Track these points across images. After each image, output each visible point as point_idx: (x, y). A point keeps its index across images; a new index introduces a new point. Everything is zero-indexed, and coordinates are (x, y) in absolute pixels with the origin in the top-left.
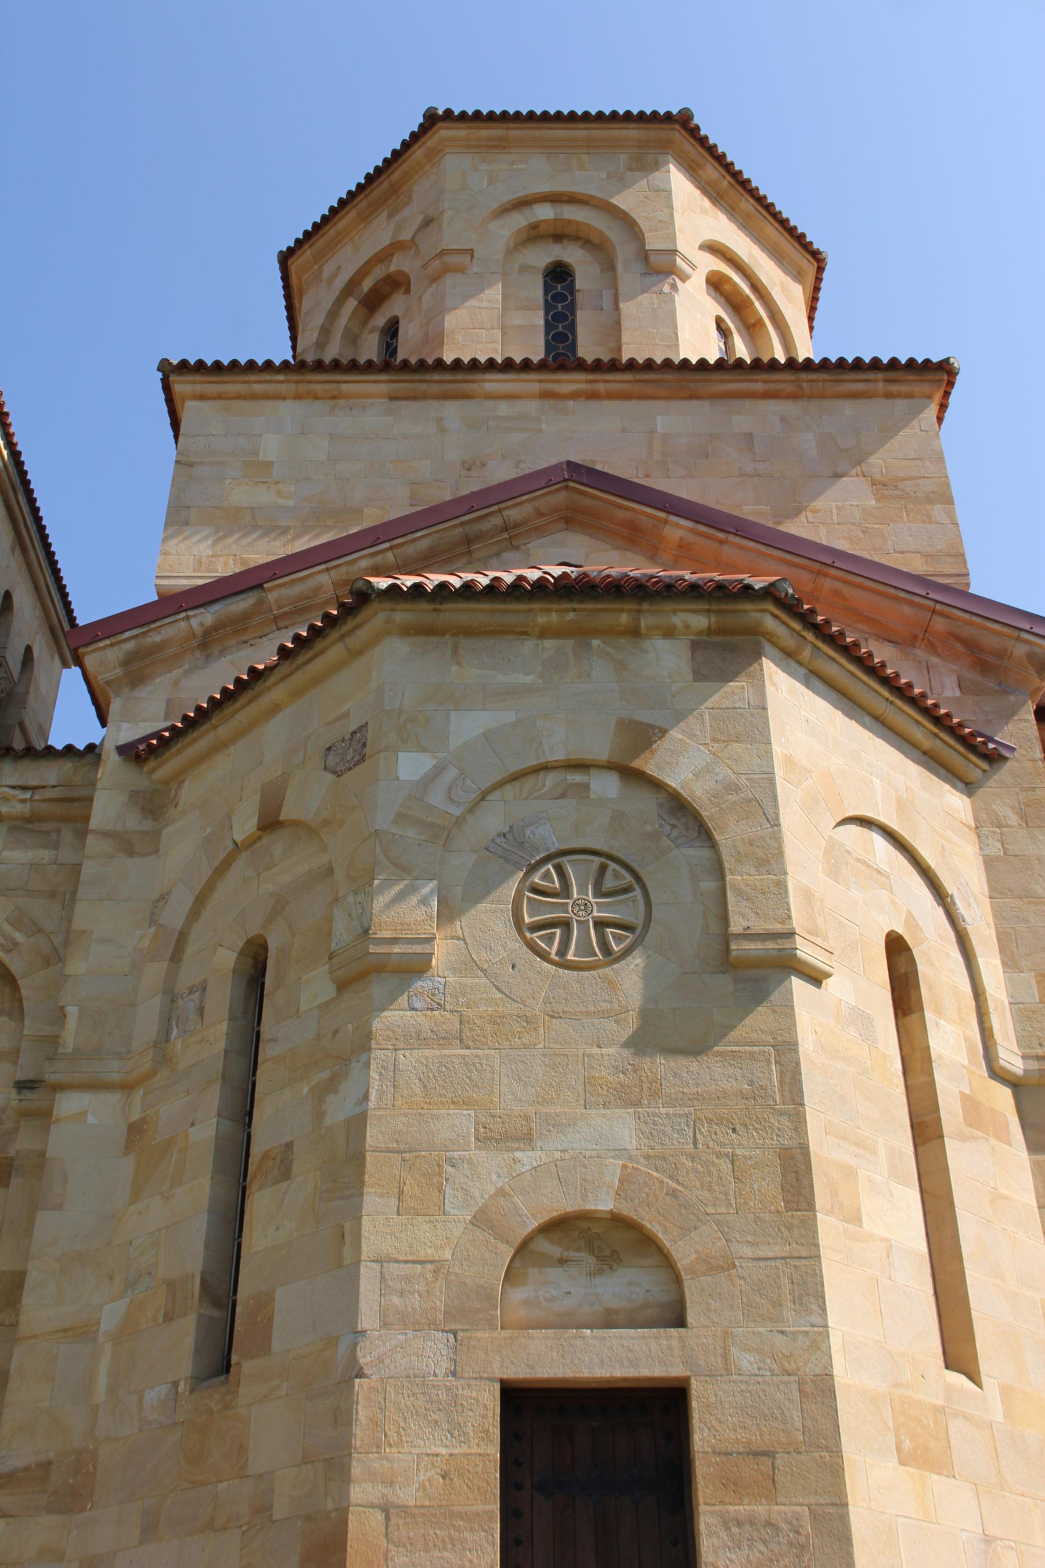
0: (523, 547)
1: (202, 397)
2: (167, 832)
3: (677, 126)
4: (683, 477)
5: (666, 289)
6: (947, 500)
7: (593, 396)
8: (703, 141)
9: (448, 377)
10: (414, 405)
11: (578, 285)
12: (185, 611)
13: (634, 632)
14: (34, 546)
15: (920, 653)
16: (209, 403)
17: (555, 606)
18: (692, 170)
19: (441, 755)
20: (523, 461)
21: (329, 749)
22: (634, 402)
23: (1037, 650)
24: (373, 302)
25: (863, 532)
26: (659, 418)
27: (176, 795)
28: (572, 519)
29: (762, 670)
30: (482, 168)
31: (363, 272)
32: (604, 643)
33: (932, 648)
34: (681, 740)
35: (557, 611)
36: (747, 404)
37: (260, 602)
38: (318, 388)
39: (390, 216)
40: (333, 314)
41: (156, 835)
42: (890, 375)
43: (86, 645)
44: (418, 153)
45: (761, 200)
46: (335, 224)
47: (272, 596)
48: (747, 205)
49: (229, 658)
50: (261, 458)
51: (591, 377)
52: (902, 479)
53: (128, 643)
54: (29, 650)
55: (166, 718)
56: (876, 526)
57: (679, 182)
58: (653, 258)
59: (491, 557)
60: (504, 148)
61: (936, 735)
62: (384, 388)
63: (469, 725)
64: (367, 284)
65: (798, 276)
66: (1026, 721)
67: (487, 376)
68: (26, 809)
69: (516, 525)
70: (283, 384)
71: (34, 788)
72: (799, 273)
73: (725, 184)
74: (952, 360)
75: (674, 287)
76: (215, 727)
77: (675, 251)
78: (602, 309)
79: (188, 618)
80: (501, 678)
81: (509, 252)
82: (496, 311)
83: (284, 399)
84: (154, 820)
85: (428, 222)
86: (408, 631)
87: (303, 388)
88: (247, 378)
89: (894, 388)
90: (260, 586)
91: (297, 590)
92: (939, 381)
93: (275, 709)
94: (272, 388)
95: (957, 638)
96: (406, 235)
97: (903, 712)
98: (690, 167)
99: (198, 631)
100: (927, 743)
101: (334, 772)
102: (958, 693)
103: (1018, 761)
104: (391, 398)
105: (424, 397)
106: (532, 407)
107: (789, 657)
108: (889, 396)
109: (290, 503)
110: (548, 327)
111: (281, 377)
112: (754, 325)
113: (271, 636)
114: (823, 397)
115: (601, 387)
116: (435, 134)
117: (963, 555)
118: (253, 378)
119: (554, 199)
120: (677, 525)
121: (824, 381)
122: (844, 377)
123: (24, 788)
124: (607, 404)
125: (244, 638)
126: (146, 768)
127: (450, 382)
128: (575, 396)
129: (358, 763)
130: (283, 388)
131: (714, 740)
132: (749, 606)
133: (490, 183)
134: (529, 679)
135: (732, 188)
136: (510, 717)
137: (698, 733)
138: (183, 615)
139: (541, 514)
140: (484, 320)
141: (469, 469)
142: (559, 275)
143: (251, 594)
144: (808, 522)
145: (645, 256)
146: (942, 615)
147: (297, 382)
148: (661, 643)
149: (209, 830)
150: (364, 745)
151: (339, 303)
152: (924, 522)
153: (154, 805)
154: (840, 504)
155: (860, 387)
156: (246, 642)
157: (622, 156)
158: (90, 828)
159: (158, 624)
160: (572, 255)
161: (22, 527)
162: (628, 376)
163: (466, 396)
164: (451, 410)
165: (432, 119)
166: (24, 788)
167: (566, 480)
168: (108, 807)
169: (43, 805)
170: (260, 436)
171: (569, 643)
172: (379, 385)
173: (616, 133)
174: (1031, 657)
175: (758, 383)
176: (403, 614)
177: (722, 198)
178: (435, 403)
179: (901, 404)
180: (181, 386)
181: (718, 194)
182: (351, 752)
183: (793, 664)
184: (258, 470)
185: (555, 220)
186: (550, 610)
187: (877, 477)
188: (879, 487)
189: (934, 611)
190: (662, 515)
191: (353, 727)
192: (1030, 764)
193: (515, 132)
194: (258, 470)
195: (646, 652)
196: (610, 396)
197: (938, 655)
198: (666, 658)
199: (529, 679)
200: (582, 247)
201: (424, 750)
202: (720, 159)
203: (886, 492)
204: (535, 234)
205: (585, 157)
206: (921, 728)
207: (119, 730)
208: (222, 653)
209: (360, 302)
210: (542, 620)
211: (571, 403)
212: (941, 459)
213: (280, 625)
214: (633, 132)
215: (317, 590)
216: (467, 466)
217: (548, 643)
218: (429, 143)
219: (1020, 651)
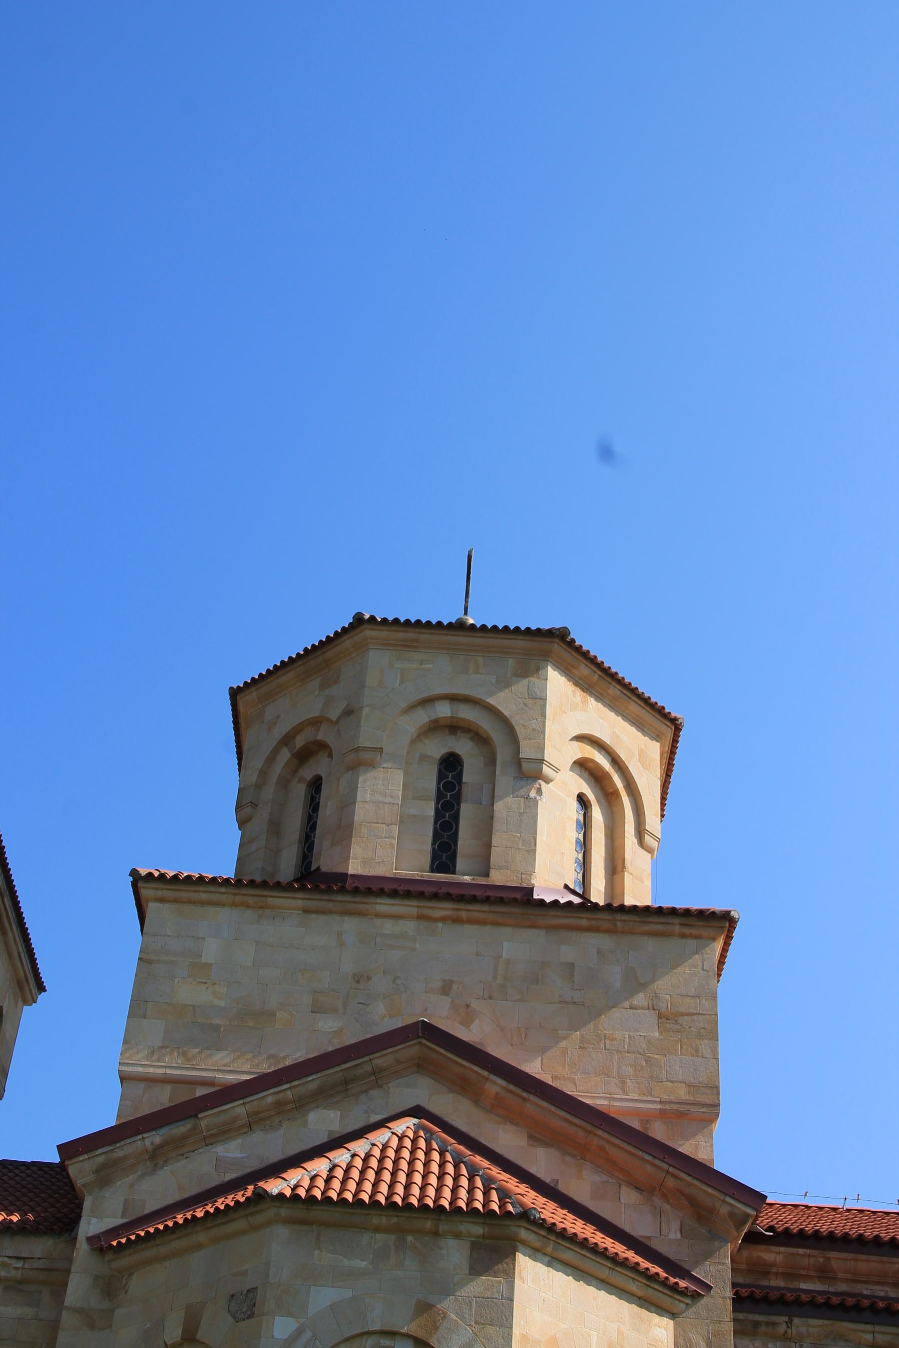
0: (385, 1086)
1: (161, 900)
2: (119, 1312)
3: (557, 640)
4: (516, 1001)
5: (533, 794)
6: (713, 1035)
7: (457, 921)
8: (579, 649)
9: (348, 898)
10: (322, 918)
11: (465, 779)
12: (142, 1133)
13: (436, 1233)
14: (12, 929)
15: (657, 1201)
16: (167, 905)
17: (385, 1213)
18: (567, 671)
19: (302, 1320)
20: (399, 978)
21: (232, 1296)
22: (488, 927)
23: (736, 1211)
24: (304, 756)
25: (646, 1061)
26: (505, 944)
27: (126, 1284)
28: (422, 1066)
29: (514, 1269)
30: (397, 666)
31: (298, 730)
32: (415, 1239)
33: (665, 1197)
34: (455, 1321)
35: (386, 1216)
36: (574, 936)
37: (195, 1128)
38: (251, 901)
39: (323, 686)
40: (271, 759)
41: (112, 1311)
42: (684, 920)
43: (70, 1158)
44: (347, 643)
45: (627, 687)
46: (278, 678)
47: (203, 1124)
48: (614, 690)
49: (170, 1167)
51: (457, 906)
52: (682, 1014)
53: (100, 1156)
55: (123, 1216)
56: (656, 1056)
57: (556, 684)
58: (524, 765)
59: (362, 1092)
60: (416, 647)
61: (648, 1286)
62: (300, 903)
63: (322, 1298)
64: (300, 741)
65: (657, 737)
66: (724, 1264)
67: (379, 900)
68: (18, 1274)
69: (381, 1070)
70: (223, 894)
71: (24, 1258)
72: (658, 736)
73: (596, 677)
74: (732, 913)
75: (539, 791)
76: (158, 1245)
77: (542, 761)
78: (481, 804)
79: (143, 1138)
80: (346, 1262)
81: (413, 742)
82: (395, 807)
83: (224, 905)
85: (349, 712)
86: (288, 1221)
87: (238, 899)
88: (197, 889)
89: (687, 931)
90: (196, 1116)
91: (221, 1118)
92: (722, 927)
93: (199, 1247)
94: (215, 897)
95: (682, 1193)
96: (334, 714)
97: (623, 1274)
98: (566, 668)
99: (150, 1148)
100: (640, 1293)
101: (234, 1317)
102: (679, 1236)
103: (712, 1297)
104: (306, 911)
105: (330, 912)
106: (409, 926)
107: (536, 1253)
108: (683, 936)
109: (222, 1003)
110: (438, 815)
111: (223, 890)
112: (612, 794)
113: (201, 1150)
114: (632, 933)
115: (464, 915)
116: (361, 632)
117: (718, 1088)
118: (201, 888)
119: (454, 699)
120: (495, 1083)
121: (634, 921)
122: (650, 919)
124: (467, 927)
125: (181, 1152)
126: (107, 1258)
127: (350, 902)
128: (443, 919)
129: (249, 1317)
130: (223, 898)
131: (476, 1323)
132: (510, 1223)
133: (402, 682)
134: (364, 1264)
135: (602, 680)
136: (348, 1293)
137: (467, 1316)
138: (140, 1137)
139: (399, 1062)
140: (382, 832)
141: (358, 982)
142: (451, 765)
143: (189, 1121)
144: (605, 1049)
145: (518, 762)
146: (674, 1176)
147: (235, 894)
148: (451, 1242)
149: (148, 1325)
150: (254, 1305)
151: (275, 751)
152: (693, 1056)
153: (110, 1288)
154: (632, 1034)
155: (660, 928)
156: (182, 1155)
157: (510, 660)
158: (65, 1304)
160: (463, 747)
162: (485, 908)
163: (361, 914)
164: (350, 926)
165: (358, 620)
166: (18, 1258)
167: (420, 1037)
168: (78, 1288)
170: (203, 939)
171: (392, 1237)
172: (295, 902)
173: (507, 642)
174: (732, 1215)
175: (583, 920)
176: (284, 1212)
177: (593, 688)
178: (337, 918)
179: (692, 942)
180: (146, 891)
181: (590, 685)
182: (247, 1306)
183: (540, 1255)
184: (200, 971)
185: (452, 718)
186: (382, 1215)
187: (663, 1011)
188: (664, 1020)
189: (668, 1172)
190: (485, 1073)
191: (249, 1288)
192: (721, 1301)
193: (424, 636)
194: (200, 971)
195: (441, 1249)
196: (470, 921)
197: (669, 1204)
198: (454, 1253)
199: (364, 1264)
200: (472, 739)
201: (291, 1315)
202: (593, 660)
203: (668, 1025)
204: (436, 727)
205: (481, 660)
206: (637, 1283)
207: (89, 1224)
208: (166, 1162)
209: (292, 755)
210: (376, 1221)
211: (440, 925)
212: (715, 997)
213: (207, 1142)
214: (521, 643)
215: (235, 1119)
216: (356, 979)
217: (380, 1237)
218: (356, 638)
219: (724, 1210)
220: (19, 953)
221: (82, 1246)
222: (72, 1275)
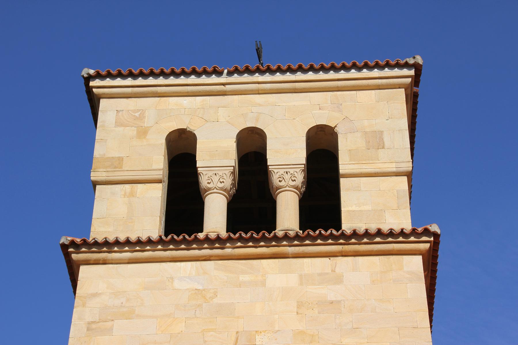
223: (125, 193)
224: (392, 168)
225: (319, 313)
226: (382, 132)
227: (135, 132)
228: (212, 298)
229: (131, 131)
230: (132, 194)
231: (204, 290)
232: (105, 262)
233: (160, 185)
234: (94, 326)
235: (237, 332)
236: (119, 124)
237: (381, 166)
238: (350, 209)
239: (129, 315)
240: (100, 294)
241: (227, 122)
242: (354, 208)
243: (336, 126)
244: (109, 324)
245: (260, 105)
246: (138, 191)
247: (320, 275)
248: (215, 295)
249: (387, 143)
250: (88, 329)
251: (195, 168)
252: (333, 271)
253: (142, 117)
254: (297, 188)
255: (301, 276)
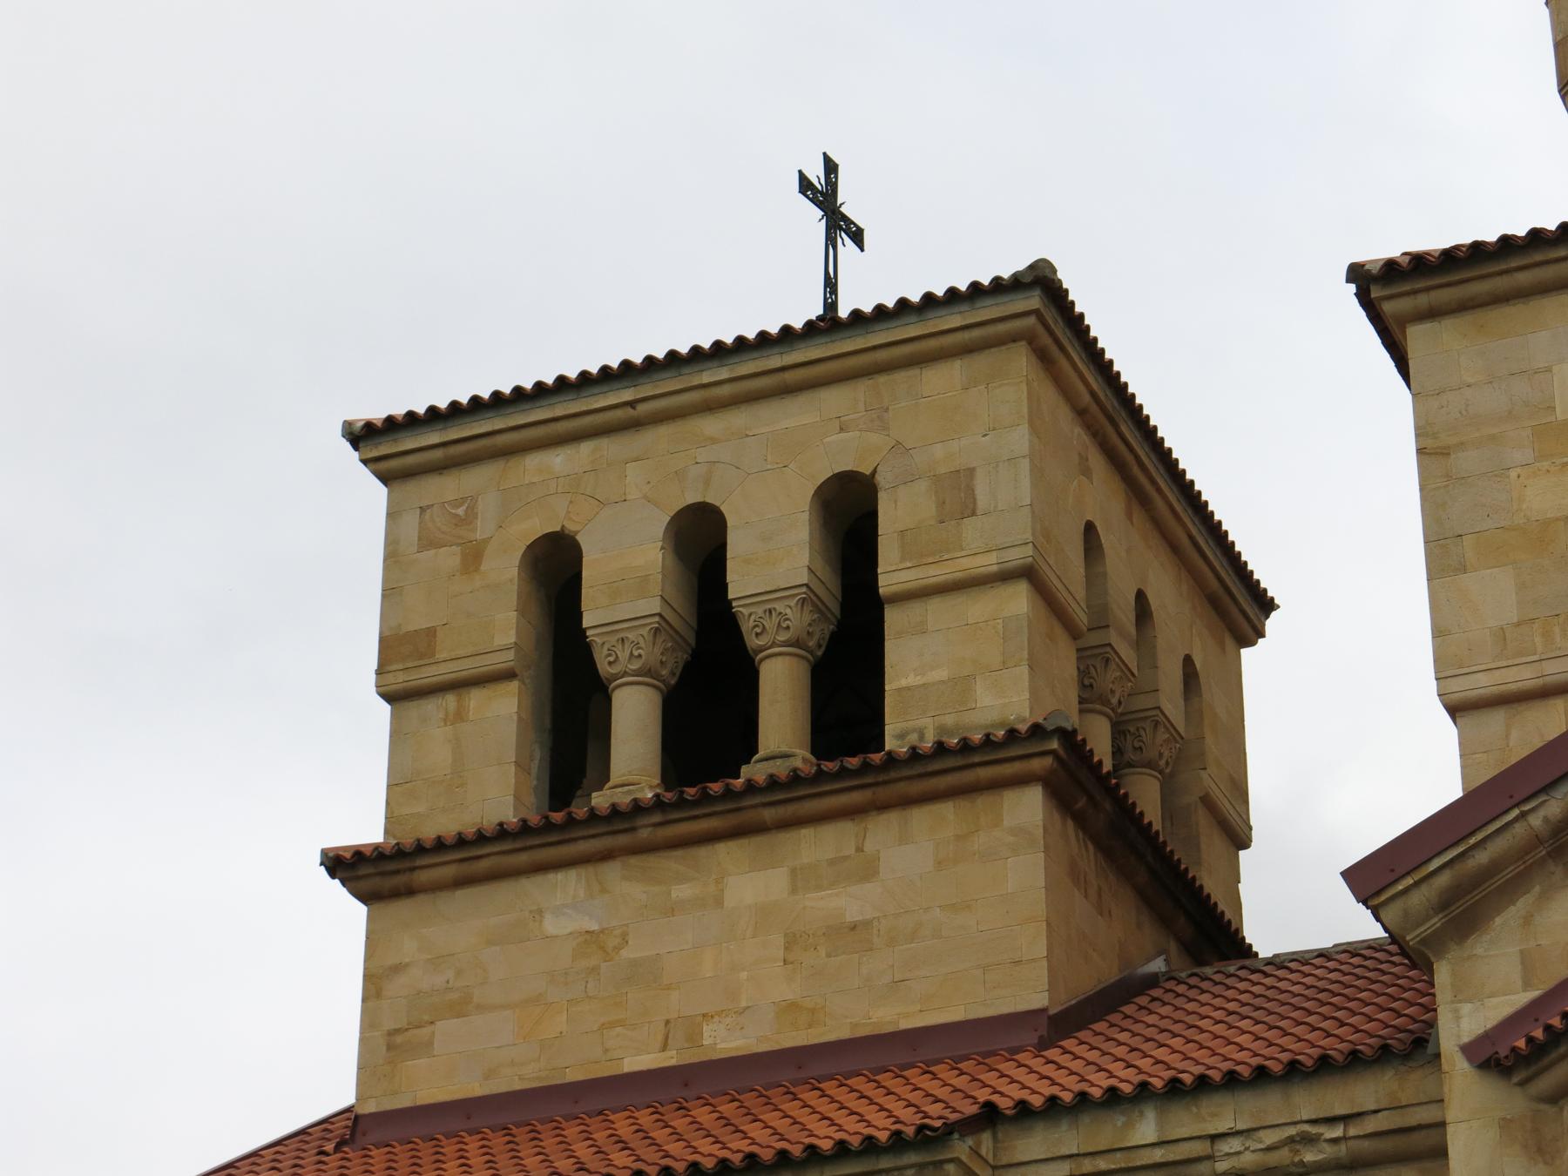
1: (1432, 314)
14: (1159, 490)
50: (1560, 414)
54: (1188, 661)
55: (1527, 985)
68: (1342, 1150)
71: (1345, 1119)
84: (1546, 1163)
123: (1331, 1121)
126: (1515, 1079)
159: (1480, 836)
161: (1136, 470)
166: (1331, 1121)
169: (1366, 1144)
170: (1549, 370)
207: (1458, 1018)
220: (1191, 538)
221: (1457, 1067)
222: (1450, 1129)
223: (447, 714)
224: (988, 563)
225: (828, 956)
226: (971, 471)
227: (458, 560)
228: (617, 949)
229: (449, 558)
230: (460, 716)
231: (602, 931)
232: (410, 892)
233: (514, 686)
234: (399, 1039)
235: (667, 1022)
236: (428, 542)
237: (966, 563)
238: (904, 683)
239: (460, 1007)
240: (407, 965)
241: (645, 497)
242: (911, 680)
243: (875, 471)
244: (426, 1031)
245: (714, 441)
246: (472, 704)
247: (832, 862)
248: (624, 939)
249: (982, 500)
250: (390, 1047)
251: (582, 633)
252: (860, 849)
253: (469, 519)
254: (796, 643)
255: (793, 871)
